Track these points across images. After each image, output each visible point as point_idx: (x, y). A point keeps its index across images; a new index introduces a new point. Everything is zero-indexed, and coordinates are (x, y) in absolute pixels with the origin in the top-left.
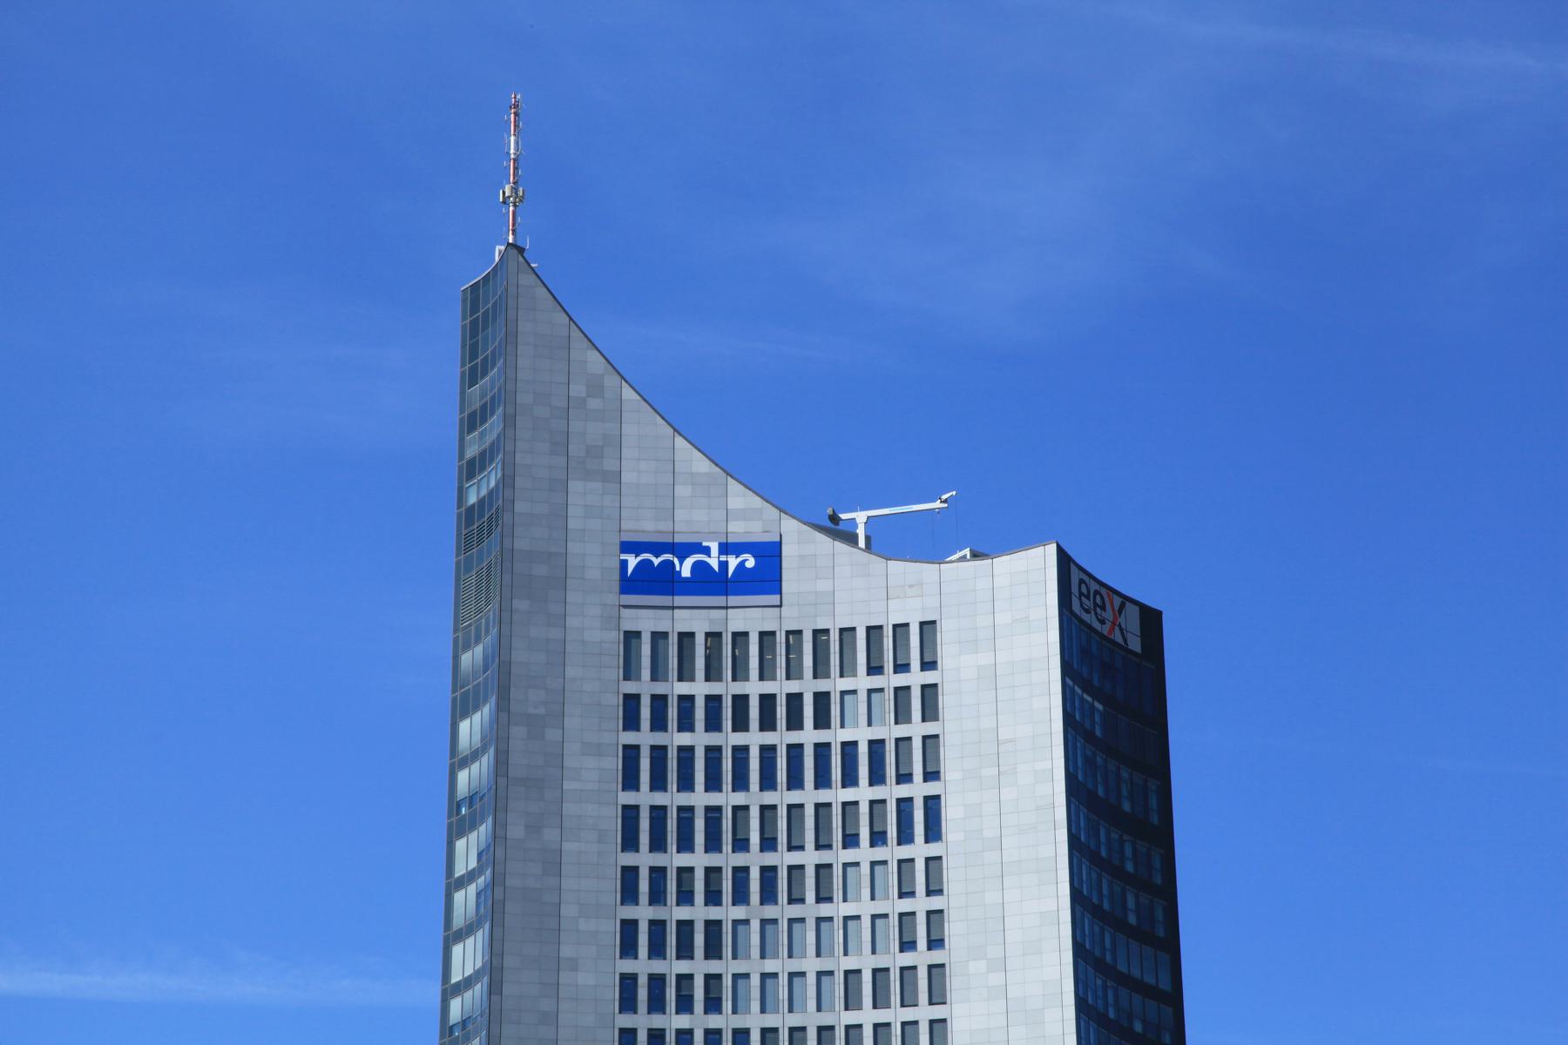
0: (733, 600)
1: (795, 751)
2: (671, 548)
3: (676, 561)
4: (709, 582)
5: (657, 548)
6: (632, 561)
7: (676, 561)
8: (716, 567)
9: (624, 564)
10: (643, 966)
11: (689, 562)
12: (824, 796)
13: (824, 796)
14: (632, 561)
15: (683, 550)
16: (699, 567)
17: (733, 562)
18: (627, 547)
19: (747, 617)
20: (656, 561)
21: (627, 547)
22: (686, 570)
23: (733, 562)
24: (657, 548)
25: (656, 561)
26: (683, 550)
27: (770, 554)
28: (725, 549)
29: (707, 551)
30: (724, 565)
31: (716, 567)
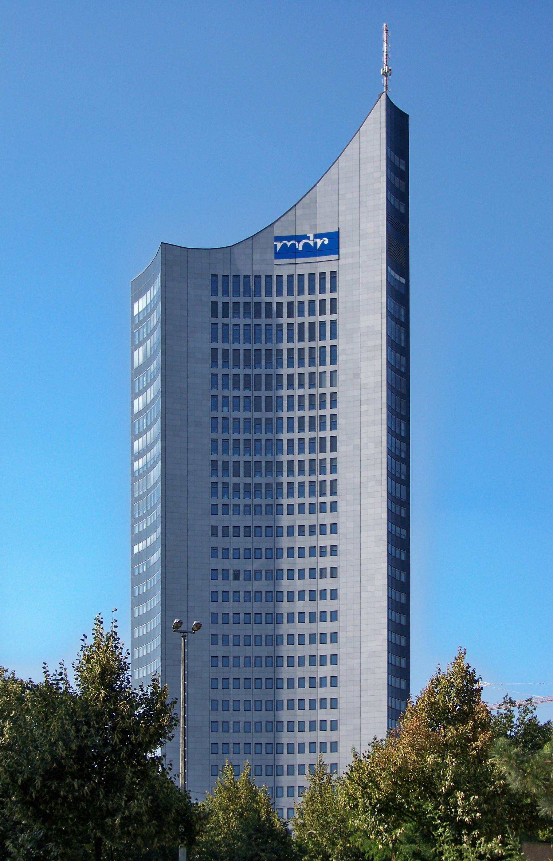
0: (320, 259)
1: (312, 291)
3: (297, 243)
4: (310, 251)
5: (289, 238)
6: (279, 245)
7: (297, 243)
8: (312, 244)
9: (276, 246)
11: (302, 243)
12: (312, 369)
13: (312, 369)
14: (279, 245)
15: (299, 238)
16: (306, 245)
17: (319, 242)
20: (289, 244)
21: (279, 239)
23: (319, 242)
25: (289, 244)
27: (334, 237)
29: (309, 238)
30: (316, 244)
31: (312, 244)
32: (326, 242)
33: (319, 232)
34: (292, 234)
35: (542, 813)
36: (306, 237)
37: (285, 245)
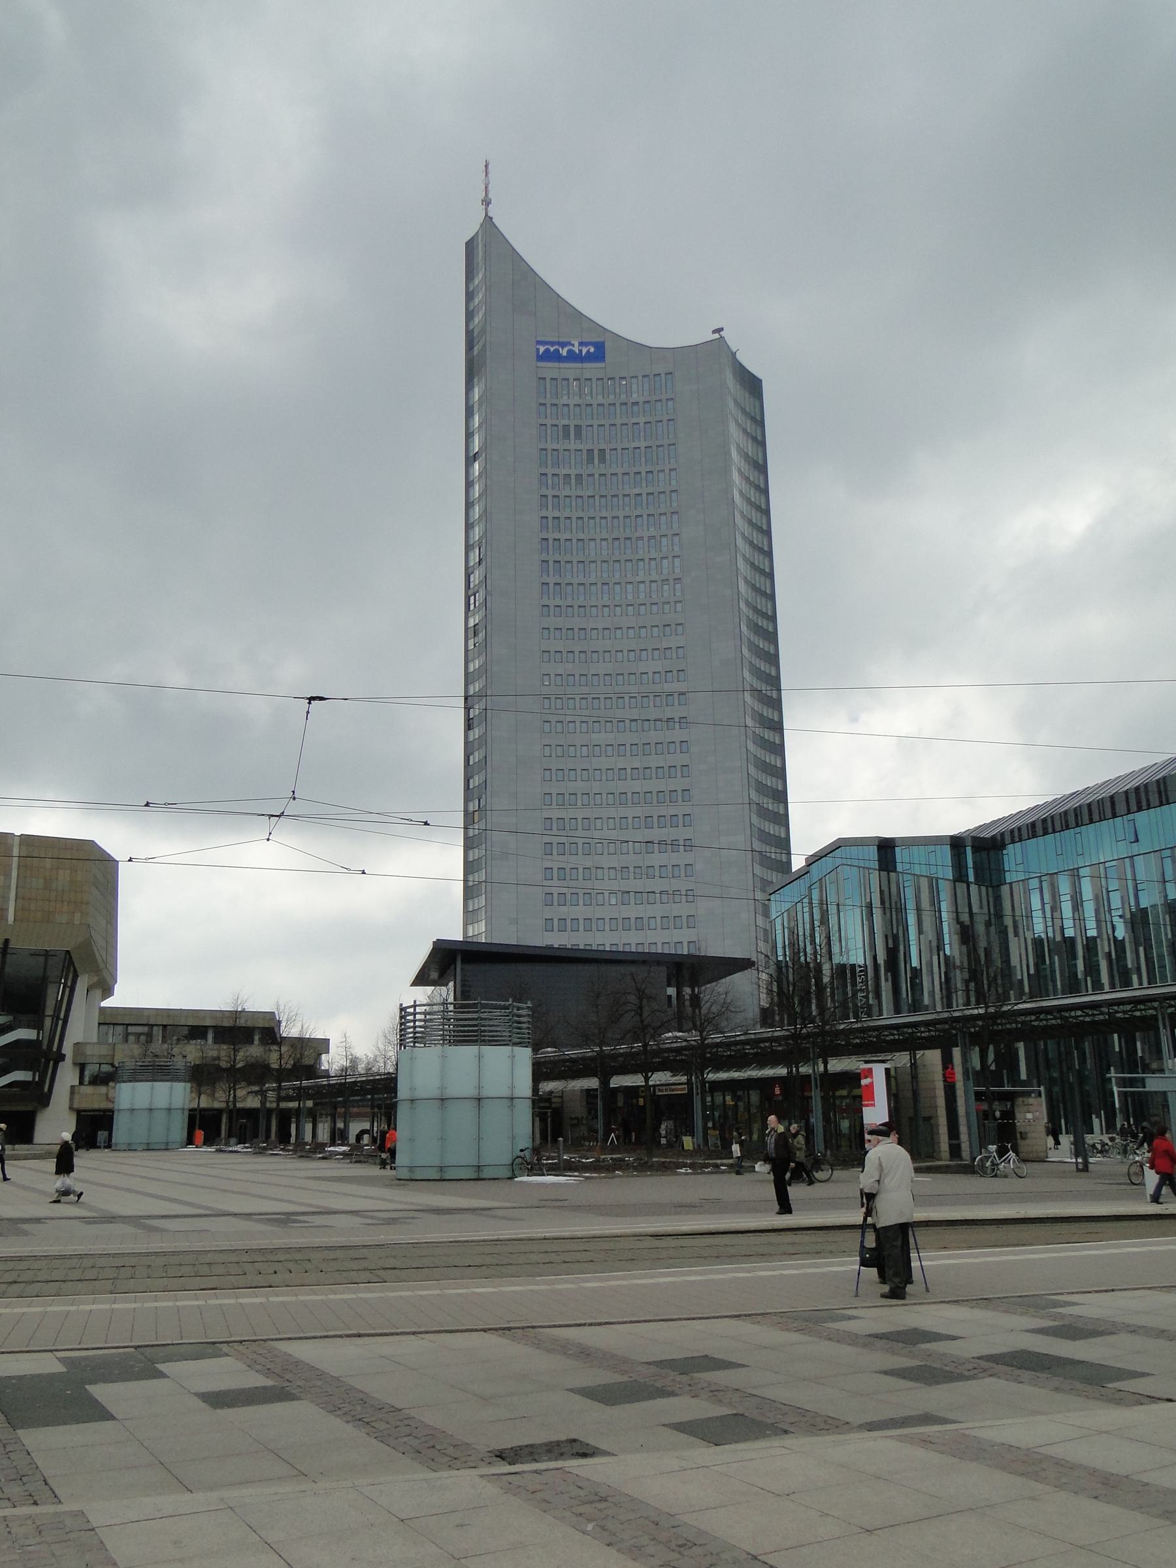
0: (586, 365)
2: (559, 344)
5: (552, 344)
6: (542, 349)
9: (538, 350)
10: (551, 514)
11: (566, 349)
16: (569, 351)
17: (584, 351)
18: (539, 343)
19: (592, 369)
20: (552, 349)
21: (539, 343)
22: (565, 354)
24: (552, 344)
25: (552, 349)
26: (563, 345)
27: (600, 347)
28: (581, 344)
30: (581, 351)
32: (592, 350)
33: (584, 340)
34: (556, 340)
35: (874, 1245)
36: (569, 343)
37: (547, 350)
